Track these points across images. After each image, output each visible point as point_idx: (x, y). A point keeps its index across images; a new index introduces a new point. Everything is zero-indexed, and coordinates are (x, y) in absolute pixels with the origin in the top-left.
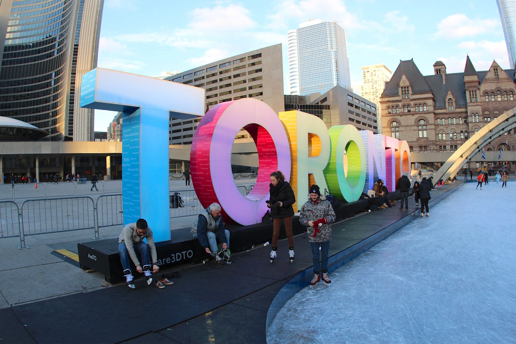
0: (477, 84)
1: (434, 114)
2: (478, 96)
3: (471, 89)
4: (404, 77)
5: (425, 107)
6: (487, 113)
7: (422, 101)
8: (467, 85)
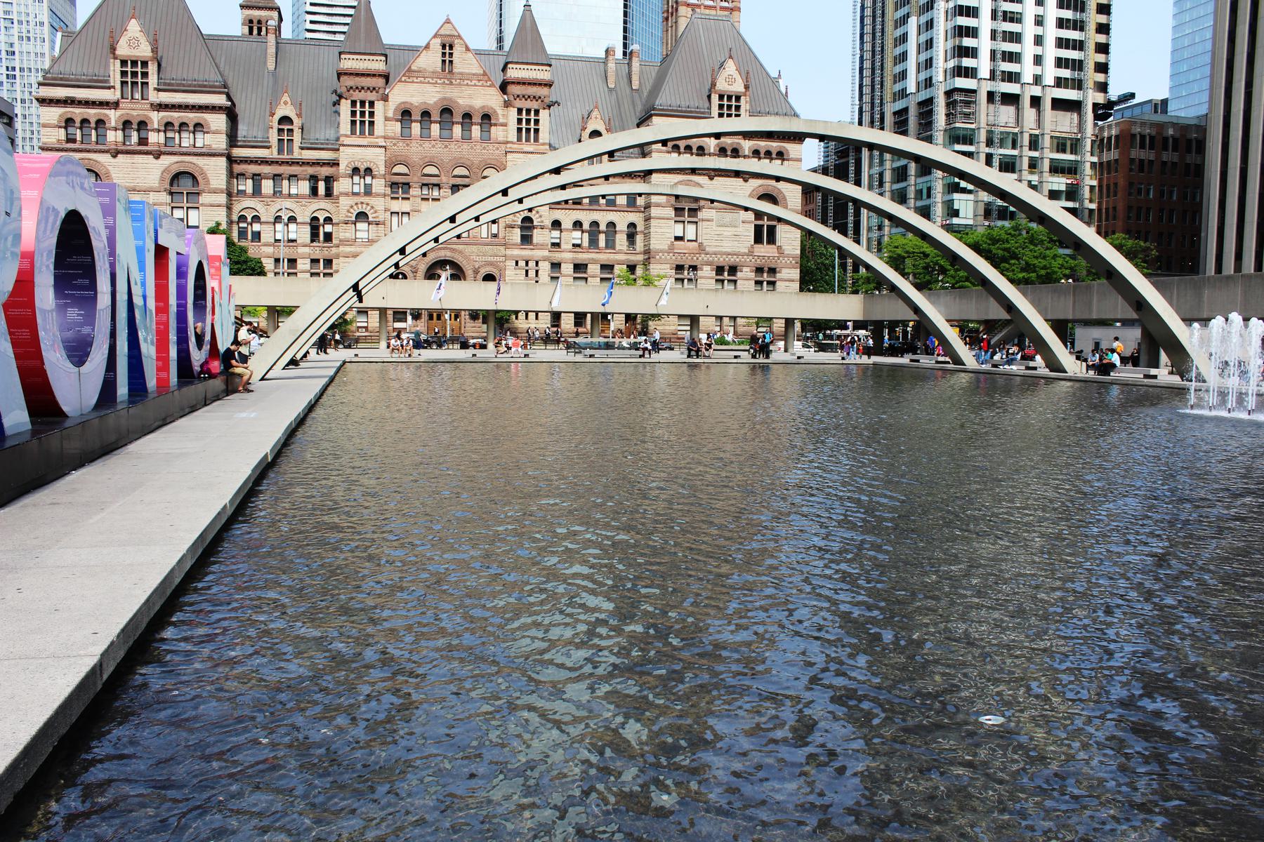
1: (231, 160)
2: (379, 119)
3: (358, 96)
4: (134, 27)
5: (199, 135)
6: (400, 169)
7: (191, 117)
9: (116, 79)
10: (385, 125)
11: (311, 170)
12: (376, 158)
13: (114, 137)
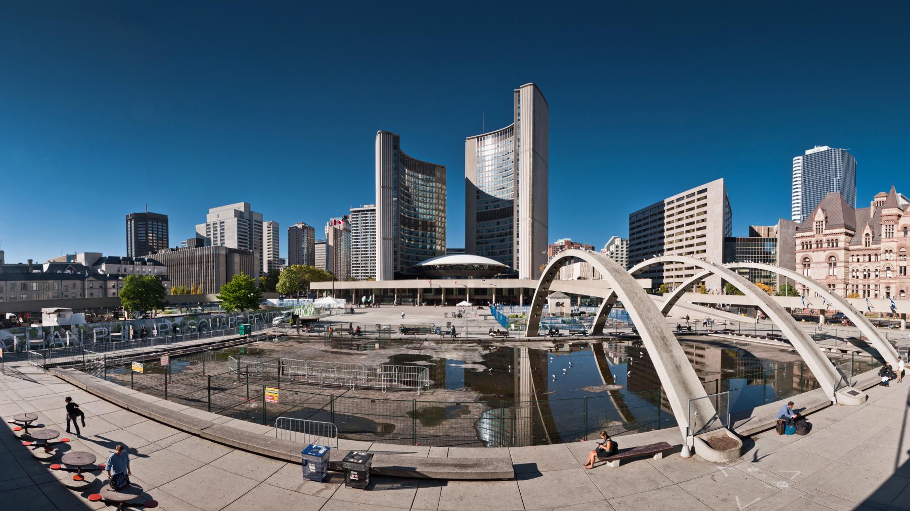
0: (896, 217)
1: (847, 249)
2: (895, 231)
8: (884, 219)
9: (814, 228)
10: (898, 233)
11: (875, 252)
12: (893, 246)
13: (814, 246)
